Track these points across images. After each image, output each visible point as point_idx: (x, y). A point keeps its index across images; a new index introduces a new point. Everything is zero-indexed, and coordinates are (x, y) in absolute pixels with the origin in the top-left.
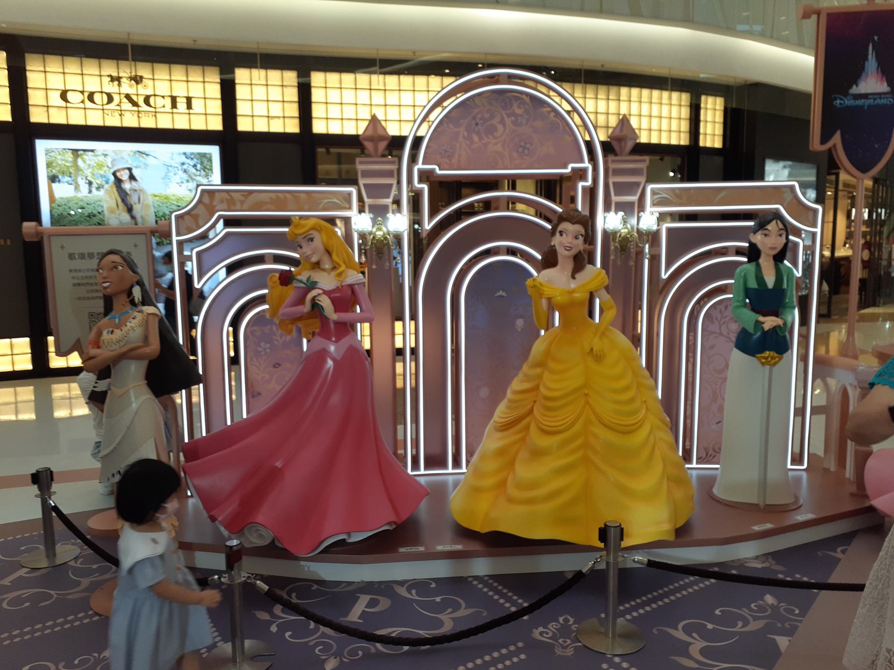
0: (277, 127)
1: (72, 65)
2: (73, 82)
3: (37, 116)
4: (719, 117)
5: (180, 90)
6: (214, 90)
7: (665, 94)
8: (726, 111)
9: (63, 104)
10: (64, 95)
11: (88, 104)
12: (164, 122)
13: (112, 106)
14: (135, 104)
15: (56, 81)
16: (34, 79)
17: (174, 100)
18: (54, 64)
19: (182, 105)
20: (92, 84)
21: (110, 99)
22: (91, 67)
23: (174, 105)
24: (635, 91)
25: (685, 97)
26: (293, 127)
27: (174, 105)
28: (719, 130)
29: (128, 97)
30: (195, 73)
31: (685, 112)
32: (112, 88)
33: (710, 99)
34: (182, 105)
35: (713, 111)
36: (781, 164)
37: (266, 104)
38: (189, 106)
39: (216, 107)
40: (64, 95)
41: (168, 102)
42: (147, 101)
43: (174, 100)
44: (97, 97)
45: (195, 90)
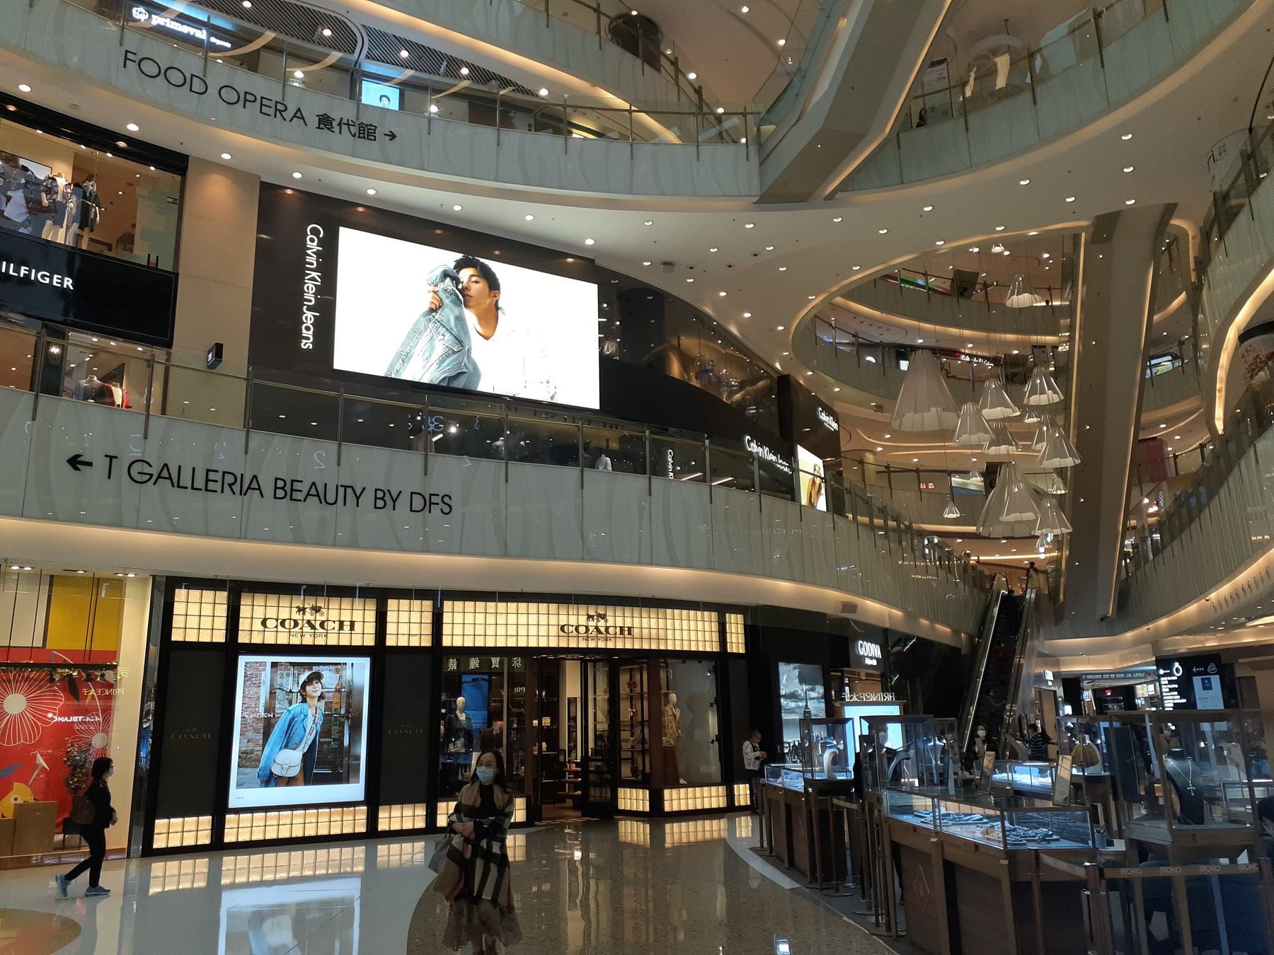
0: (415, 642)
1: (272, 600)
2: (271, 613)
3: (243, 638)
4: (741, 630)
5: (346, 617)
6: (371, 616)
7: (699, 613)
8: (746, 627)
9: (262, 628)
10: (264, 623)
11: (280, 628)
12: (332, 641)
13: (297, 629)
14: (313, 627)
15: (259, 613)
16: (245, 611)
17: (341, 624)
18: (259, 599)
19: (347, 628)
20: (284, 614)
21: (296, 624)
22: (285, 601)
23: (341, 627)
24: (677, 612)
25: (714, 615)
26: (427, 642)
27: (341, 627)
28: (741, 639)
29: (309, 622)
30: (358, 603)
31: (715, 626)
32: (296, 616)
33: (733, 616)
34: (347, 628)
35: (735, 625)
36: (792, 666)
37: (408, 626)
38: (352, 628)
39: (371, 628)
40: (264, 623)
41: (337, 625)
42: (322, 625)
43: (341, 624)
44: (287, 623)
45: (358, 616)
